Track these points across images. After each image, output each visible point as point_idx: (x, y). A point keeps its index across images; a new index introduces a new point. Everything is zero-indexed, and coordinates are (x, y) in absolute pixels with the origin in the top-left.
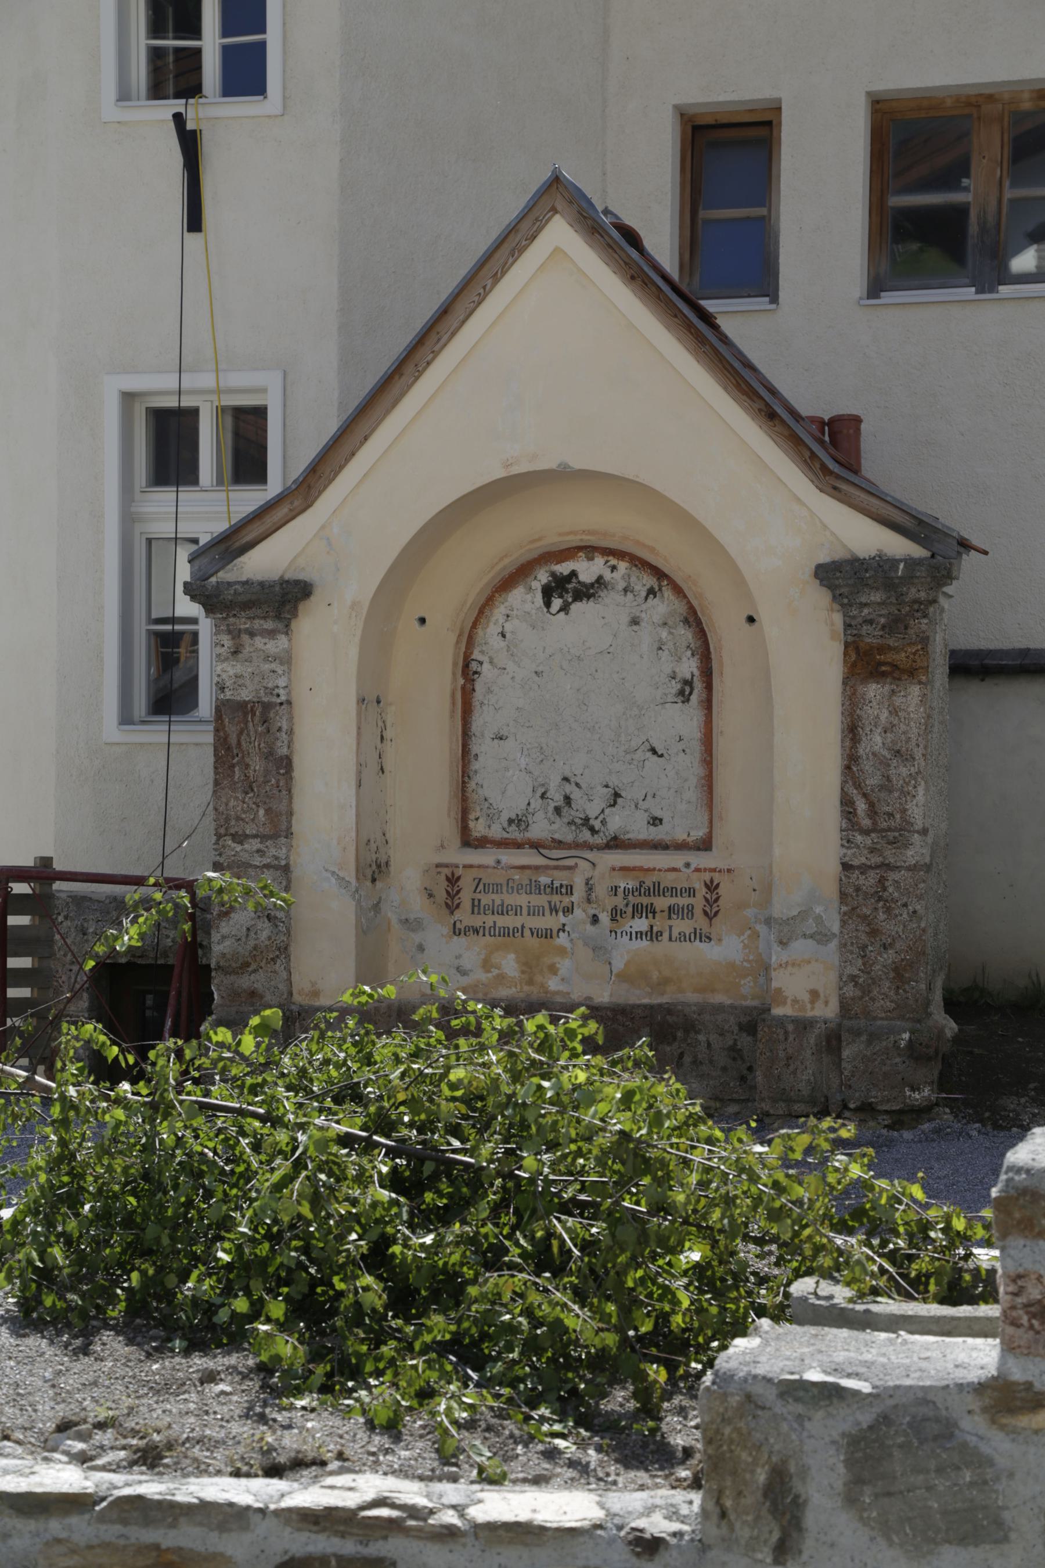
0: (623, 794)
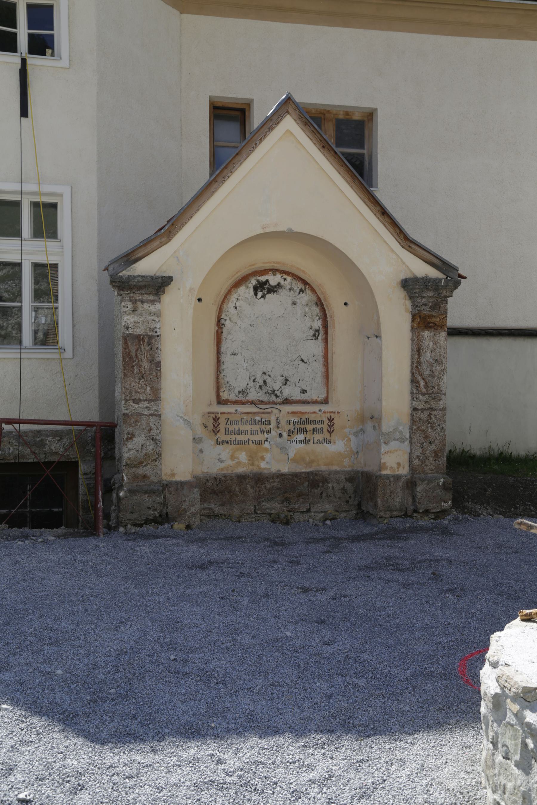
0: (289, 380)
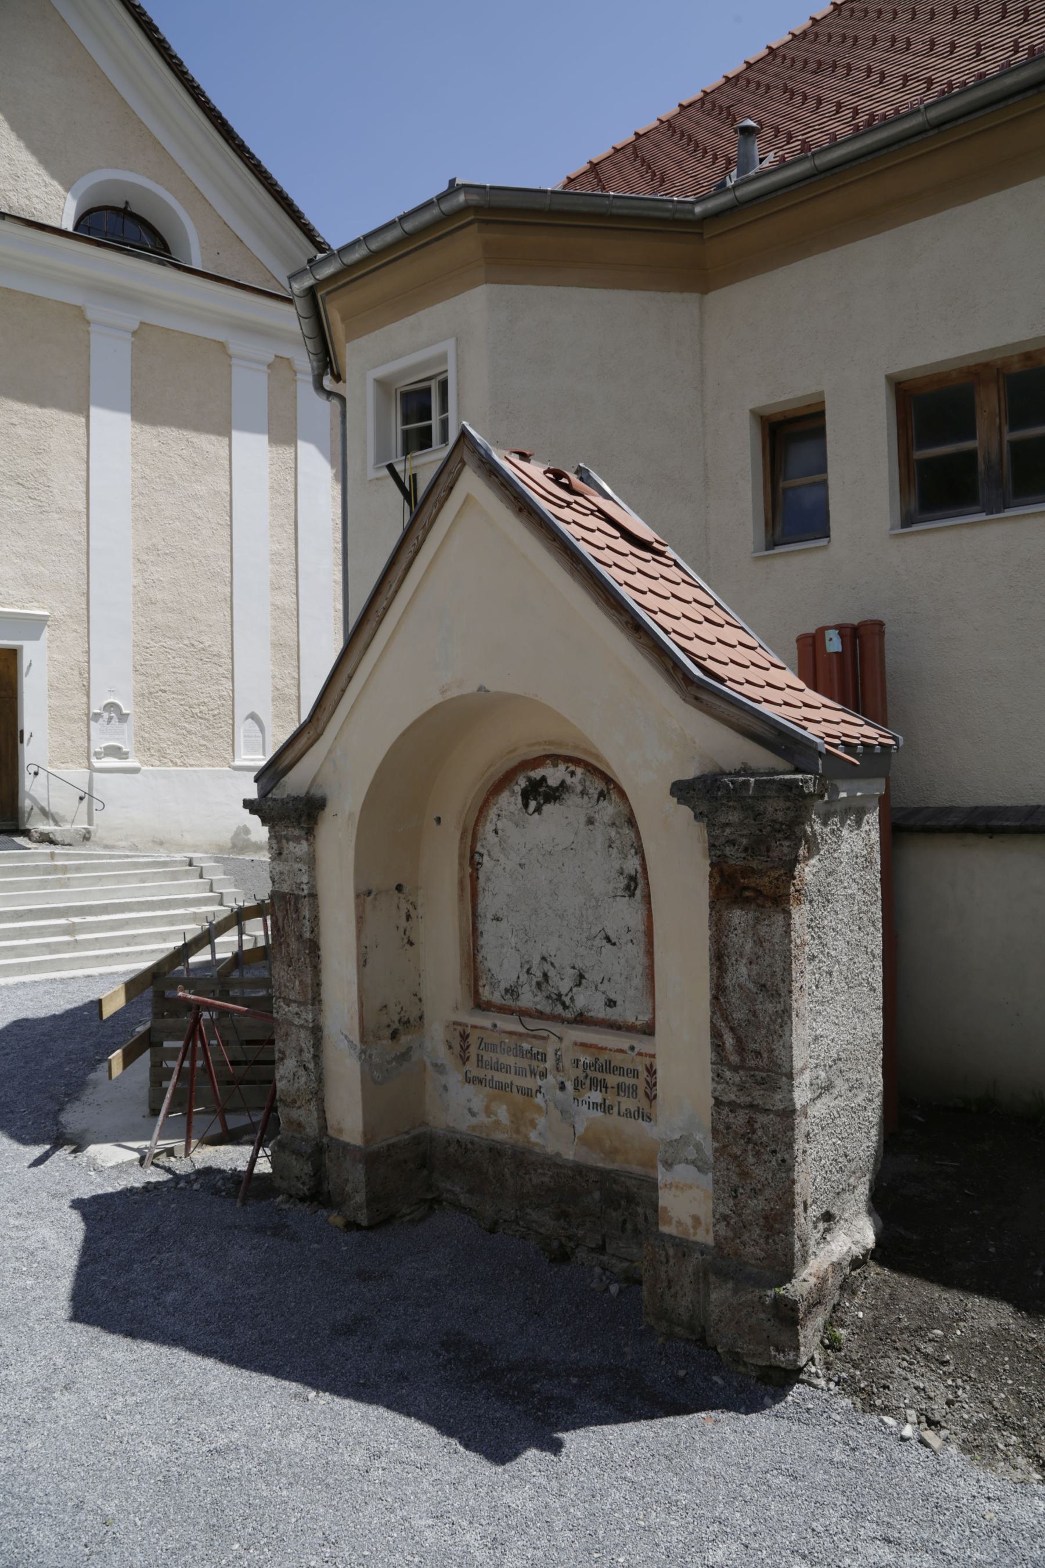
0: (587, 976)
